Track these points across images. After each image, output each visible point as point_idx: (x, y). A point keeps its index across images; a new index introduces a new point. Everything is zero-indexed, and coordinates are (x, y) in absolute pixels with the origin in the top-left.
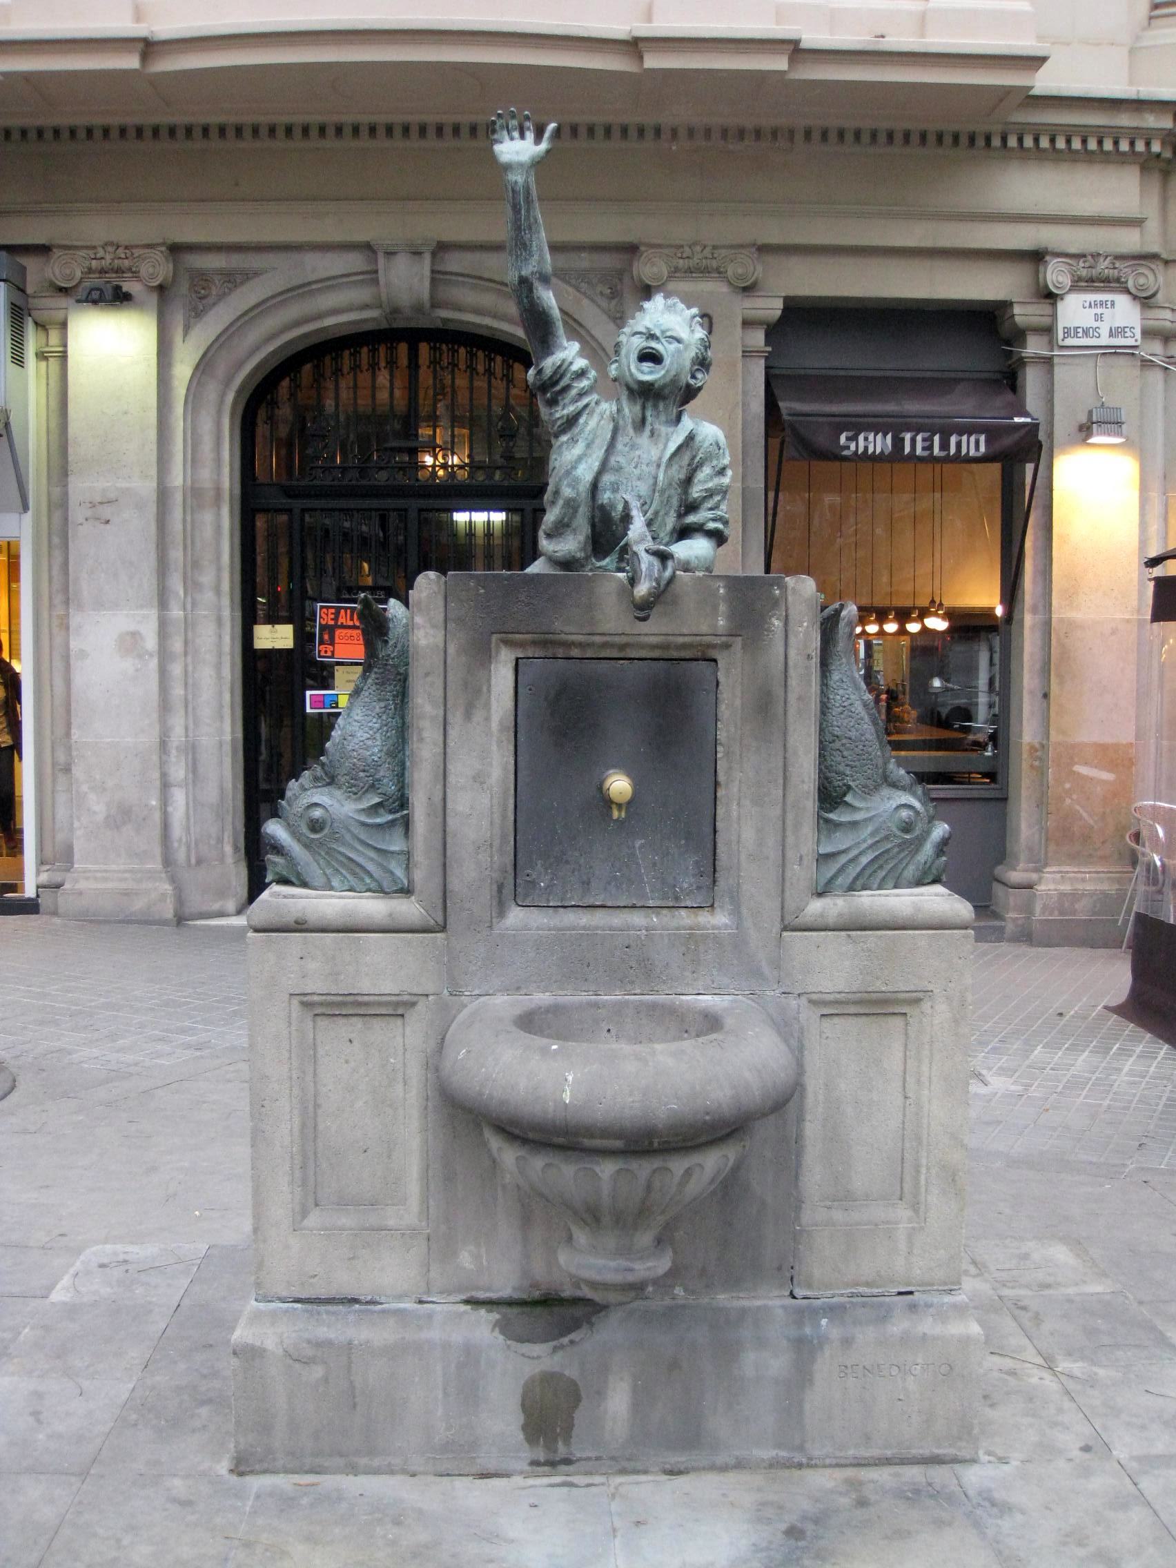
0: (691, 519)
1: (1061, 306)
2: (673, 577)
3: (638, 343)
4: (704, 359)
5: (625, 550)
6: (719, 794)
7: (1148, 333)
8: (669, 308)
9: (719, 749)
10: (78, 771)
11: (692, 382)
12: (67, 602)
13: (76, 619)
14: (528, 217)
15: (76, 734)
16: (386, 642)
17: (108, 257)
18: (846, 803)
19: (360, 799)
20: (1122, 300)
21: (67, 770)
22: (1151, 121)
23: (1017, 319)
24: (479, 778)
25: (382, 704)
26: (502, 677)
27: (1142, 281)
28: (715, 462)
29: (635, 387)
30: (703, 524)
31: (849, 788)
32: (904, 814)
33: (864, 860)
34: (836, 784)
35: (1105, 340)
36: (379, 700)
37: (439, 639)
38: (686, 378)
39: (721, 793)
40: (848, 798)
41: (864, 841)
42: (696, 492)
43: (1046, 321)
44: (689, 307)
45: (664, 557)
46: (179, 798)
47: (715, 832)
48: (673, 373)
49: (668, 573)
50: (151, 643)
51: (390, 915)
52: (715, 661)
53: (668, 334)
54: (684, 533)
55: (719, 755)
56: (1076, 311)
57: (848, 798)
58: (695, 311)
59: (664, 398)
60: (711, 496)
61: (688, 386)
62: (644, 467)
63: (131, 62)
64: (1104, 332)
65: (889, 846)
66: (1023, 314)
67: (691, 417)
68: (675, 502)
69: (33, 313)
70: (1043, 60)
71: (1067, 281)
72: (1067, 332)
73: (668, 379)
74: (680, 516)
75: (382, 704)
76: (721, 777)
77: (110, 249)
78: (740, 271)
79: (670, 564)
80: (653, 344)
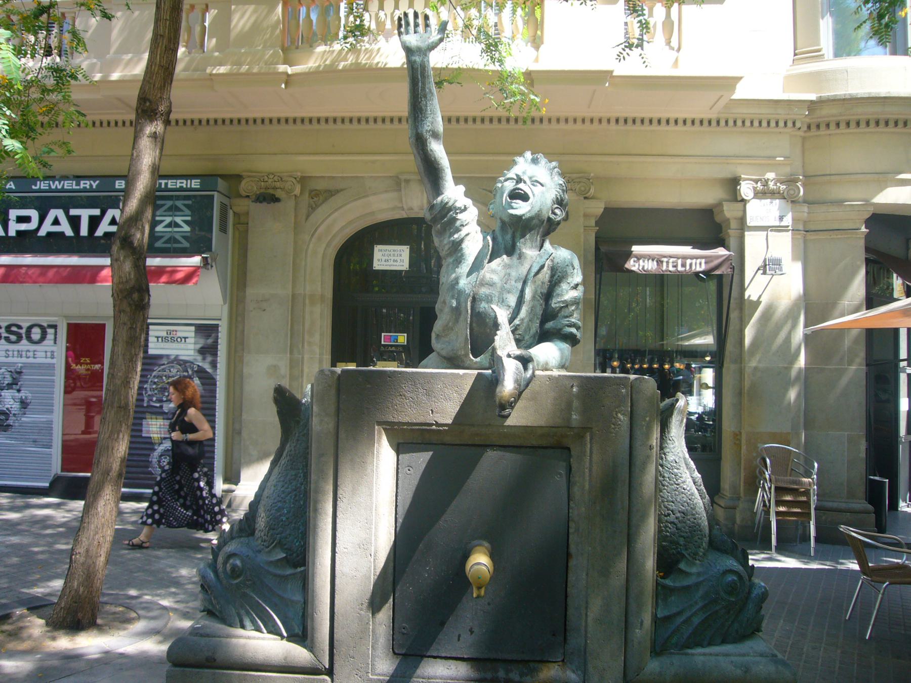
0: (550, 325)
1: (748, 206)
2: (533, 375)
3: (509, 186)
4: (562, 200)
5: (494, 349)
6: (570, 564)
8: (535, 161)
9: (572, 524)
10: (245, 434)
11: (552, 216)
12: (243, 350)
13: (247, 358)
14: (423, 89)
15: (244, 416)
16: (298, 422)
17: (270, 181)
18: (680, 569)
19: (270, 552)
21: (240, 433)
23: (726, 212)
24: (364, 546)
25: (293, 473)
27: (792, 192)
28: (570, 280)
29: (506, 219)
30: (561, 329)
31: (683, 556)
32: (730, 578)
33: (696, 621)
34: (671, 552)
36: (291, 468)
37: (331, 426)
38: (547, 213)
39: (571, 563)
40: (682, 566)
41: (696, 603)
42: (555, 303)
43: (740, 214)
44: (550, 161)
45: (525, 361)
47: (566, 597)
48: (537, 209)
49: (529, 373)
51: (285, 658)
52: (569, 449)
53: (534, 179)
54: (544, 336)
55: (571, 531)
57: (682, 566)
58: (554, 164)
59: (530, 230)
60: (567, 306)
61: (549, 219)
62: (513, 283)
65: (717, 608)
66: (730, 211)
67: (551, 244)
68: (539, 311)
69: (235, 208)
70: (741, 78)
71: (751, 195)
73: (533, 213)
74: (543, 322)
75: (293, 473)
76: (573, 549)
77: (271, 176)
78: (583, 189)
79: (530, 366)
80: (521, 186)
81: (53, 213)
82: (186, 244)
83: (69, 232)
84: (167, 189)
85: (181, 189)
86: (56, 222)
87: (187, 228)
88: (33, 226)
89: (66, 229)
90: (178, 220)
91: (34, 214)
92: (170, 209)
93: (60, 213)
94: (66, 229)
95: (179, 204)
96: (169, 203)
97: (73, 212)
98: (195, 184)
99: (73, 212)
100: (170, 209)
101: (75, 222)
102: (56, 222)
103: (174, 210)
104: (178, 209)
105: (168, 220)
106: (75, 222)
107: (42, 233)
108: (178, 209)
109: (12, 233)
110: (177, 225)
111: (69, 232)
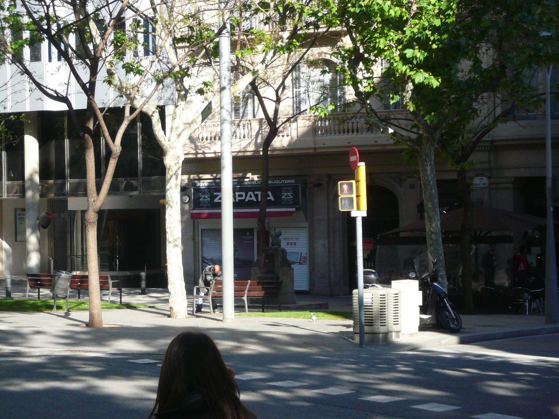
7: (490, 184)
20: (484, 178)
22: (486, 144)
26: (264, 254)
35: (482, 186)
46: (332, 273)
50: (327, 246)
56: (477, 180)
63: (312, 151)
64: (482, 184)
72: (476, 185)
81: (250, 193)
82: (291, 203)
83: (255, 200)
84: (285, 184)
85: (289, 183)
86: (251, 196)
87: (292, 197)
88: (243, 198)
89: (254, 198)
90: (289, 194)
91: (243, 194)
92: (286, 190)
93: (250, 193)
94: (254, 198)
95: (289, 188)
96: (286, 188)
97: (256, 193)
98: (293, 181)
99: (256, 193)
100: (286, 190)
101: (256, 196)
102: (251, 196)
103: (287, 191)
104: (289, 190)
105: (286, 194)
106: (256, 196)
107: (247, 200)
108: (289, 190)
109: (237, 201)
110: (289, 196)
111: (255, 200)
